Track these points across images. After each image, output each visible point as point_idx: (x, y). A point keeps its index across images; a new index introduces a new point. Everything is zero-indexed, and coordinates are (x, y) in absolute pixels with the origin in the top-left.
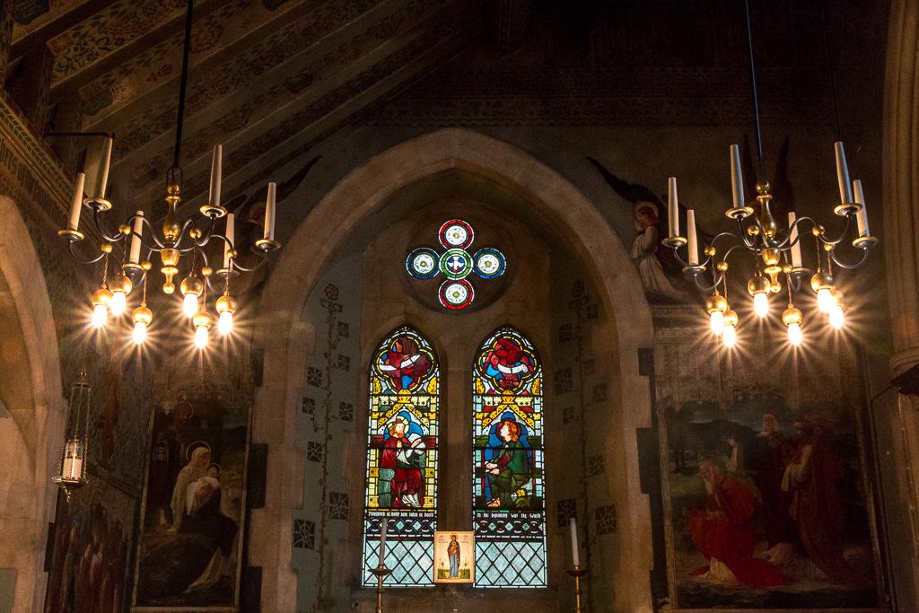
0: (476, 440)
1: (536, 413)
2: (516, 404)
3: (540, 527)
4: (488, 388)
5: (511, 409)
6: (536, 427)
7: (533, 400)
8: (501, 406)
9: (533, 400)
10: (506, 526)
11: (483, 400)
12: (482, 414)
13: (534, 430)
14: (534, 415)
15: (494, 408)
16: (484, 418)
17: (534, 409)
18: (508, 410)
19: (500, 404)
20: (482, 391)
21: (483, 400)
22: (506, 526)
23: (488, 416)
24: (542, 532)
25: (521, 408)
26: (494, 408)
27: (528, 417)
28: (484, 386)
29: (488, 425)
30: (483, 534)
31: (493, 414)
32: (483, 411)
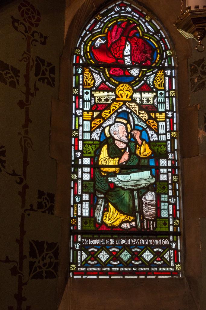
0: (83, 145)
1: (161, 113)
2: (134, 101)
3: (167, 256)
4: (98, 81)
5: (127, 107)
6: (163, 129)
7: (156, 96)
8: (116, 104)
9: (156, 96)
10: (144, 256)
11: (92, 95)
12: (90, 114)
13: (158, 134)
14: (158, 115)
15: (107, 106)
16: (93, 119)
17: (157, 108)
18: (124, 108)
19: (114, 100)
20: (91, 84)
21: (92, 95)
22: (122, 256)
23: (99, 116)
24: (170, 262)
25: (142, 107)
26: (107, 106)
27: (150, 117)
28: (94, 78)
29: (99, 127)
30: (115, 266)
31: (106, 113)
32: (92, 110)
